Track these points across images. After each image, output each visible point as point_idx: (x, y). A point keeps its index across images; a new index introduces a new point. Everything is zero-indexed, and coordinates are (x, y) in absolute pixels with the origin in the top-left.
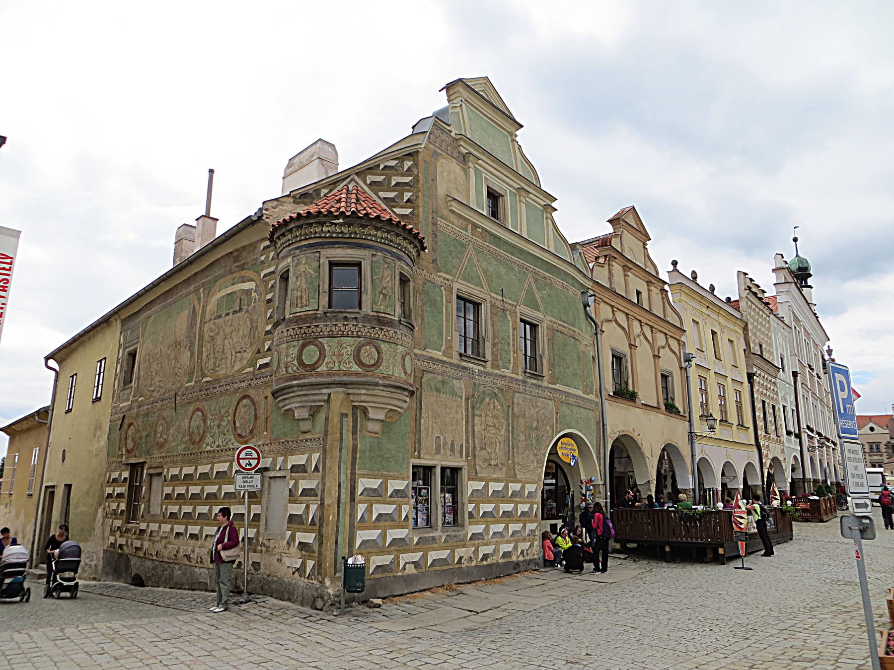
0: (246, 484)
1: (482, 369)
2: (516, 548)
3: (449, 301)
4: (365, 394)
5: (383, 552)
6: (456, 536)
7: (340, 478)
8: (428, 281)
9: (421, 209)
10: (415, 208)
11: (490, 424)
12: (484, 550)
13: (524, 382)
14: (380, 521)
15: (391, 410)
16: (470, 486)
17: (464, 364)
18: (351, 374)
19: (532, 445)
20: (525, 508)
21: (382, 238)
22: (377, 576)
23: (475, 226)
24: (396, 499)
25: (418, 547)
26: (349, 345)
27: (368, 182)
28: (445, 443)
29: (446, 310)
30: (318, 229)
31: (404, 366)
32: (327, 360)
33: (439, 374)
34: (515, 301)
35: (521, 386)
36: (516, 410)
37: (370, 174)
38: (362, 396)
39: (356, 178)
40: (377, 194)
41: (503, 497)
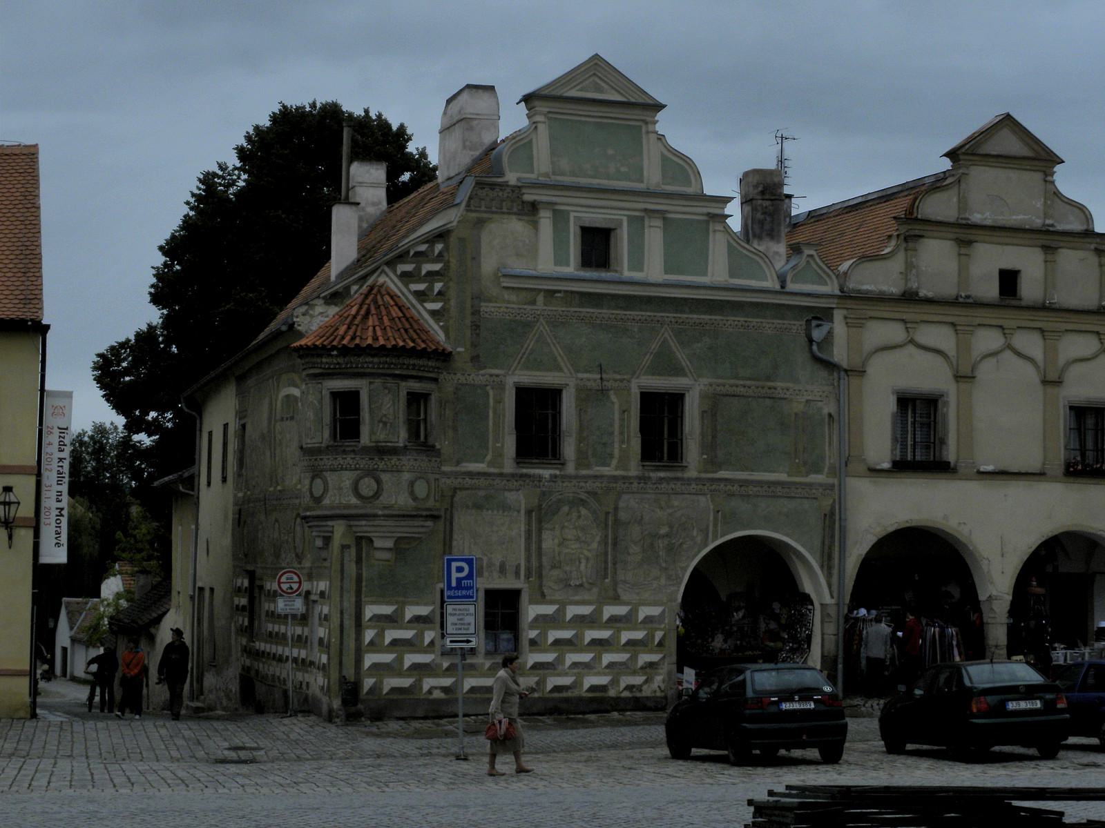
0: (288, 607)
1: (557, 472)
2: (614, 682)
3: (499, 401)
4: (365, 526)
5: (400, 674)
8: (462, 385)
9: (453, 302)
10: (446, 301)
11: (569, 537)
12: (552, 682)
13: (642, 479)
14: (395, 645)
15: (399, 538)
16: (531, 611)
17: (525, 471)
18: (348, 507)
20: (639, 635)
22: (391, 697)
23: (550, 293)
25: (448, 673)
26: (347, 479)
27: (399, 273)
29: (495, 413)
30: (319, 360)
31: (412, 493)
32: (330, 493)
35: (635, 485)
36: (623, 515)
38: (363, 527)
40: (406, 286)
41: (593, 622)
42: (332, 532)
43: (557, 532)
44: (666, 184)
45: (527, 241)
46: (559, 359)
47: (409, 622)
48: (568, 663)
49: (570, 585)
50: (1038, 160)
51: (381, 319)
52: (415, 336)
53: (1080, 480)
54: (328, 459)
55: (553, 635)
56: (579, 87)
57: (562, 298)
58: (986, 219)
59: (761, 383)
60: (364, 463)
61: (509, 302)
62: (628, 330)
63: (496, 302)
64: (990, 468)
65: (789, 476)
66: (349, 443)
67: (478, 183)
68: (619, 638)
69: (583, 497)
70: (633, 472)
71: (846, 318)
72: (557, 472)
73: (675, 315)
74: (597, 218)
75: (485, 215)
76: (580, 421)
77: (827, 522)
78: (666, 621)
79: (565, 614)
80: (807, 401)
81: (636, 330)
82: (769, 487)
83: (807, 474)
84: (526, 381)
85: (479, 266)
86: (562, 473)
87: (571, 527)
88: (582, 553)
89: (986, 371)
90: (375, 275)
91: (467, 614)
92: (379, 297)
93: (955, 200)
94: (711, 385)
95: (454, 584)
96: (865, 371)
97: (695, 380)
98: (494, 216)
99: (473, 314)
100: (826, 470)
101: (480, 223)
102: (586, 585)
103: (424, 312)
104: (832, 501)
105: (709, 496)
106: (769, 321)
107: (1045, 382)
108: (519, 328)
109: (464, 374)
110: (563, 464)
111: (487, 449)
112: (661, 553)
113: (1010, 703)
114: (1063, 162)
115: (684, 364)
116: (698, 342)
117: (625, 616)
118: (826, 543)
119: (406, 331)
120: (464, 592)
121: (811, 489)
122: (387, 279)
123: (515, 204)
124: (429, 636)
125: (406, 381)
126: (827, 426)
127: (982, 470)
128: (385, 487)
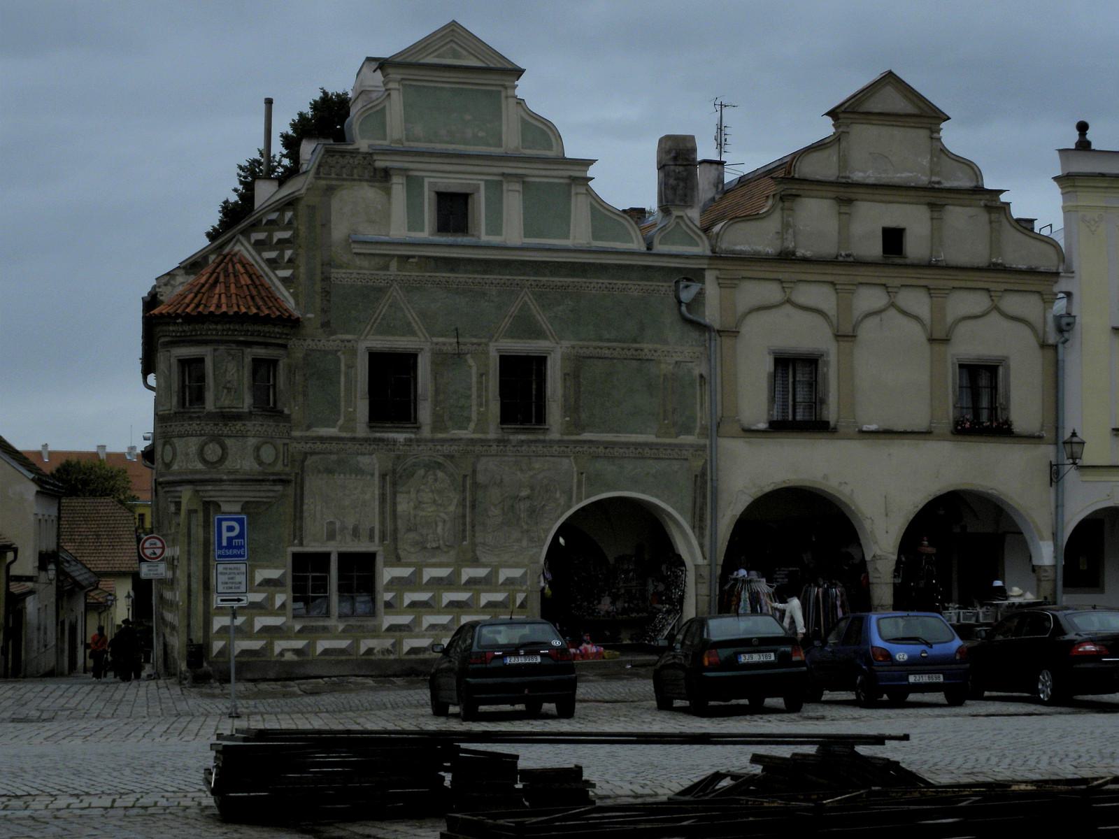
1: (413, 436)
6: (360, 626)
7: (189, 569)
9: (302, 270)
10: (296, 268)
12: (408, 644)
15: (247, 502)
16: (386, 574)
17: (378, 435)
20: (499, 597)
21: (223, 330)
24: (266, 588)
26: (193, 444)
27: (253, 241)
28: (343, 529)
31: (258, 458)
33: (331, 453)
36: (481, 478)
37: (255, 232)
38: (211, 492)
39: (241, 237)
41: (451, 584)
42: (180, 497)
43: (413, 495)
45: (379, 207)
46: (414, 324)
47: (260, 585)
48: (425, 625)
49: (426, 548)
50: (925, 117)
51: (227, 288)
52: (261, 303)
53: (969, 438)
54: (176, 426)
55: (409, 597)
56: (436, 54)
57: (416, 263)
58: (869, 177)
59: (625, 345)
60: (209, 428)
61: (361, 268)
62: (484, 294)
63: (346, 268)
64: (873, 427)
65: (657, 437)
66: (196, 408)
67: (327, 151)
68: (478, 599)
70: (492, 435)
71: (718, 278)
72: (413, 436)
73: (535, 278)
74: (453, 182)
75: (334, 183)
77: (699, 483)
78: (528, 583)
79: (421, 578)
80: (676, 362)
81: (494, 293)
82: (636, 449)
83: (677, 435)
84: (379, 346)
86: (418, 436)
89: (868, 331)
90: (232, 244)
91: (238, 574)
92: (230, 265)
93: (835, 158)
94: (573, 347)
95: (224, 543)
96: (738, 332)
98: (345, 183)
99: (323, 280)
100: (697, 431)
101: (330, 190)
103: (275, 279)
104: (703, 461)
105: (572, 458)
106: (635, 283)
107: (932, 340)
108: (373, 293)
109: (313, 340)
110: (418, 428)
111: (339, 415)
112: (522, 516)
113: (742, 656)
114: (949, 118)
115: (544, 326)
117: (484, 578)
119: (253, 298)
120: (235, 551)
121: (680, 450)
122: (242, 248)
123: (366, 171)
124: (279, 599)
125: (250, 347)
126: (698, 388)
127: (864, 429)
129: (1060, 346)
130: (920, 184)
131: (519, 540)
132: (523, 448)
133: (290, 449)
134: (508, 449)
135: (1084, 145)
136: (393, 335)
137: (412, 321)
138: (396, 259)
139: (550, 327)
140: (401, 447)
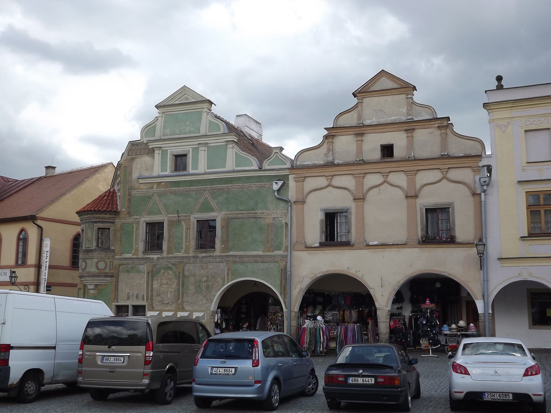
1: (160, 256)
3: (137, 229)
8: (124, 223)
11: (164, 283)
13: (194, 257)
19: (202, 291)
28: (133, 295)
29: (136, 233)
34: (189, 213)
36: (186, 273)
43: (159, 281)
44: (210, 132)
46: (161, 210)
49: (164, 303)
58: (374, 122)
64: (376, 243)
65: (263, 252)
69: (171, 266)
70: (191, 255)
72: (160, 256)
74: (179, 150)
75: (134, 156)
76: (169, 234)
78: (205, 319)
82: (253, 258)
83: (273, 251)
85: (132, 176)
87: (165, 279)
88: (168, 289)
93: (356, 116)
94: (226, 214)
97: (219, 213)
98: (139, 156)
99: (128, 195)
100: (283, 248)
101: (132, 160)
102: (171, 303)
104: (284, 263)
107: (407, 197)
108: (147, 198)
116: (221, 197)
118: (283, 283)
125: (96, 223)
127: (370, 244)
128: (88, 265)
129: (483, 194)
130: (402, 121)
131: (201, 300)
132: (204, 260)
133: (114, 263)
134: (198, 260)
135: (500, 87)
136: (153, 215)
137: (161, 208)
138: (156, 184)
139: (216, 206)
140: (155, 261)
